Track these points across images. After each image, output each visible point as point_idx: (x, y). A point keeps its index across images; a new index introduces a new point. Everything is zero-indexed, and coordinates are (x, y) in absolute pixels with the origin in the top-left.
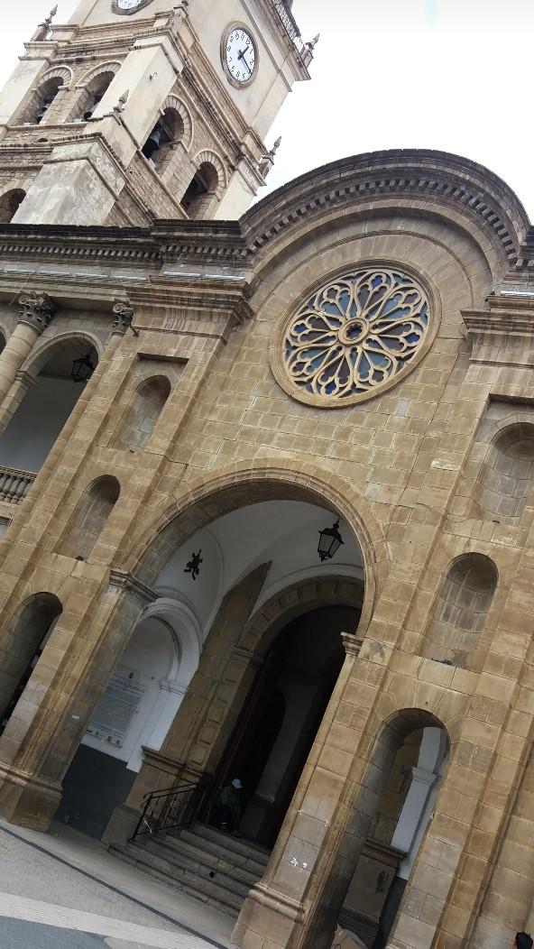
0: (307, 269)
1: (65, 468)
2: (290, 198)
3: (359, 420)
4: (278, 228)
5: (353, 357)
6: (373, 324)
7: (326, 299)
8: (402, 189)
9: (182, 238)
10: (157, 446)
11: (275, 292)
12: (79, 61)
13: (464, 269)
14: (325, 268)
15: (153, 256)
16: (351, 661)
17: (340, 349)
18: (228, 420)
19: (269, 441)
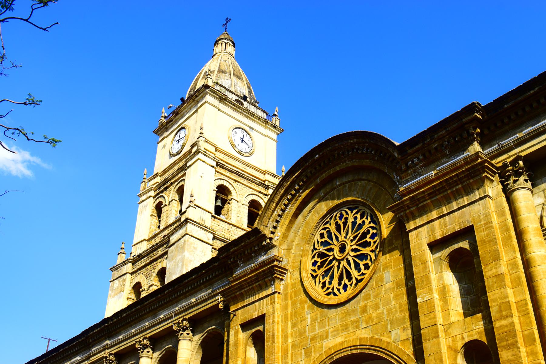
0: (303, 230)
2: (276, 200)
3: (367, 297)
4: (278, 219)
5: (349, 262)
6: (350, 240)
7: (320, 240)
12: (166, 189)
13: (380, 185)
14: (312, 225)
17: (339, 263)
18: (301, 337)
19: (327, 337)
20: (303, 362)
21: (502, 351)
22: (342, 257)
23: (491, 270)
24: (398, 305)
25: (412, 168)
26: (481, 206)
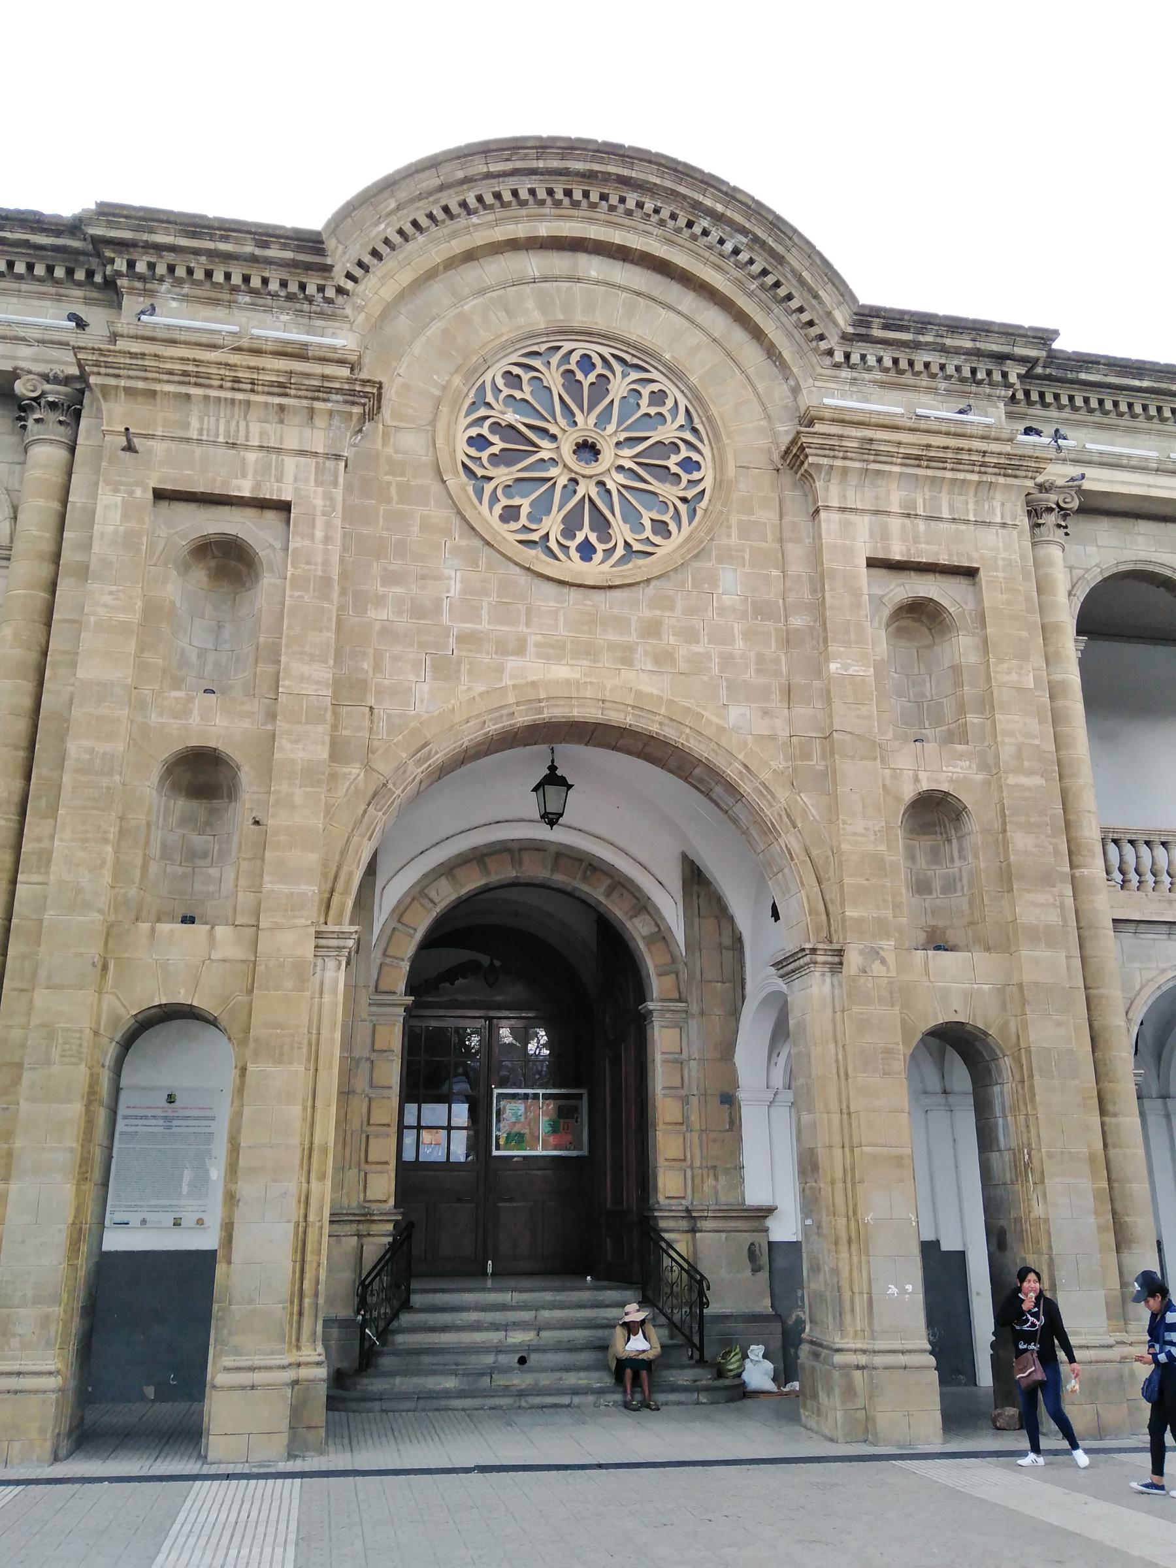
0: (446, 331)
1: (86, 743)
2: (403, 194)
3: (666, 603)
4: (383, 249)
6: (615, 440)
8: (593, 206)
9: (172, 248)
10: (302, 678)
11: (401, 371)
14: (485, 335)
15: (80, 275)
16: (824, 981)
17: (575, 481)
18: (419, 619)
19: (520, 649)
20: (426, 687)
21: (1014, 832)
22: (587, 472)
23: (1010, 673)
24: (752, 655)
25: (852, 367)
26: (1001, 540)
